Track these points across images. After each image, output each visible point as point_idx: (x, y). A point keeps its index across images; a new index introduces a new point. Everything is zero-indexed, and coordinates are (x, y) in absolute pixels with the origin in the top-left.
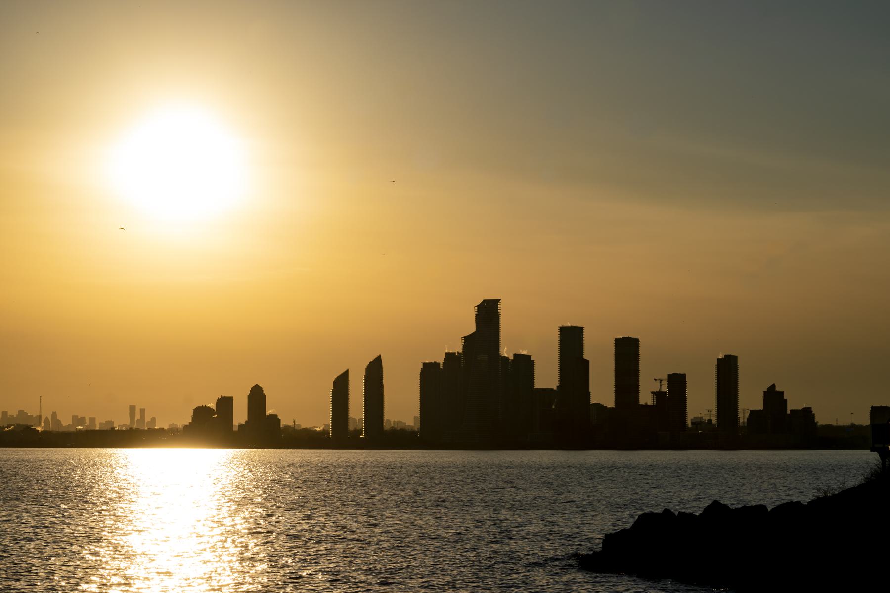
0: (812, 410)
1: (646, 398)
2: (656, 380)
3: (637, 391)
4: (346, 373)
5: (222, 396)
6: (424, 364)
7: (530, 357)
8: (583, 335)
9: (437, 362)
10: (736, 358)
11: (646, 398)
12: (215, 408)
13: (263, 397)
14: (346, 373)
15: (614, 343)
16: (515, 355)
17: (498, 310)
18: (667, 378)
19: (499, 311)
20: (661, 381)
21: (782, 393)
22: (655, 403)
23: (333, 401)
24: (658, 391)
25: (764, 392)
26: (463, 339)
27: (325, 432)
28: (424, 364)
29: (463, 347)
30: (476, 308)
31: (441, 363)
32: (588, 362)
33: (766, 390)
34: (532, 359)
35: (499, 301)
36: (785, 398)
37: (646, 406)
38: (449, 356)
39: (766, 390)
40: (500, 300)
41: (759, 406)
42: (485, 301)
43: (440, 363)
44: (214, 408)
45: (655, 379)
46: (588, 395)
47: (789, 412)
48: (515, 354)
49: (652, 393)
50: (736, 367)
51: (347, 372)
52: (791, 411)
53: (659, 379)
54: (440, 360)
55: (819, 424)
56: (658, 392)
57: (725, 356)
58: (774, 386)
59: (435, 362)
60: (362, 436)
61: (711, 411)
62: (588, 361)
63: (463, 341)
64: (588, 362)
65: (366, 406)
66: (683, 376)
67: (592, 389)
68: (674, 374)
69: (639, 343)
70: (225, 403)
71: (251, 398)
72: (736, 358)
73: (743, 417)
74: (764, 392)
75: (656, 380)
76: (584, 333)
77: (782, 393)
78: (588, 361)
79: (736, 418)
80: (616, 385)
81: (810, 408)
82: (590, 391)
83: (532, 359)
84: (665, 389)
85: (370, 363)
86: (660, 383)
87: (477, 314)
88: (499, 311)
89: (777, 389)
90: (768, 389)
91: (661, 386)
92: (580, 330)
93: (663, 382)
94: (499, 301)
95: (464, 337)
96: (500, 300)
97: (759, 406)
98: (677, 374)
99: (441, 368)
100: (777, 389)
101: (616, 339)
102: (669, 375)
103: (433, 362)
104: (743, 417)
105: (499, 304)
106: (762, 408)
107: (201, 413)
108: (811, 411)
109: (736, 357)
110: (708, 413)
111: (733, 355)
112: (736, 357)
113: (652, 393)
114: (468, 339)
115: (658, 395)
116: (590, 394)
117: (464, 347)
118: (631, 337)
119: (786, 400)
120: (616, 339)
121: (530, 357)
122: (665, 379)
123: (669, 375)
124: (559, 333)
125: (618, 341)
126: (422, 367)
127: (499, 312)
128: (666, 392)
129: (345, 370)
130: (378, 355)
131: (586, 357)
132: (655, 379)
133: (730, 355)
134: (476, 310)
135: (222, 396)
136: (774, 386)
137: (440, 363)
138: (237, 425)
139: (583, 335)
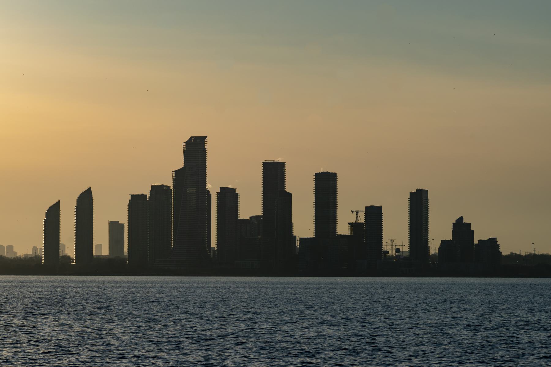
0: (497, 240)
2: (353, 212)
3: (335, 222)
4: (57, 205)
6: (132, 196)
7: (235, 189)
8: (284, 170)
14: (57, 205)
15: (314, 177)
16: (221, 188)
18: (364, 210)
19: (205, 147)
20: (357, 213)
21: (470, 224)
22: (352, 233)
23: (45, 230)
24: (354, 222)
25: (453, 224)
26: (174, 173)
27: (36, 258)
28: (132, 196)
30: (185, 144)
31: (148, 196)
32: (290, 195)
33: (455, 222)
35: (205, 137)
36: (472, 229)
37: (345, 236)
38: (157, 190)
39: (455, 222)
40: (207, 137)
41: (449, 237)
42: (191, 137)
43: (146, 196)
45: (352, 211)
46: (291, 225)
47: (476, 242)
48: (222, 187)
49: (349, 224)
51: (59, 202)
52: (479, 241)
54: (147, 192)
55: (503, 254)
57: (417, 190)
58: (462, 218)
59: (143, 194)
60: (72, 263)
61: (393, 241)
62: (291, 194)
63: (174, 175)
64: (290, 195)
65: (77, 235)
67: (293, 220)
68: (371, 206)
69: (337, 177)
73: (434, 247)
74: (453, 224)
75: (353, 212)
76: (285, 168)
77: (470, 224)
78: (291, 194)
79: (427, 248)
80: (315, 217)
81: (496, 238)
82: (292, 222)
84: (362, 220)
86: (357, 214)
87: (184, 150)
88: (205, 147)
89: (465, 221)
90: (456, 221)
91: (357, 217)
92: (282, 165)
93: (359, 214)
94: (205, 137)
96: (207, 137)
97: (449, 237)
98: (373, 206)
99: (148, 199)
100: (465, 221)
102: (366, 207)
103: (140, 194)
104: (434, 247)
105: (205, 140)
106: (452, 240)
108: (497, 242)
109: (427, 191)
110: (391, 242)
112: (427, 191)
113: (349, 224)
114: (177, 172)
115: (355, 226)
116: (292, 225)
117: (175, 181)
119: (473, 231)
121: (235, 189)
122: (361, 211)
123: (366, 208)
124: (262, 168)
125: (317, 175)
126: (130, 199)
127: (206, 148)
128: (363, 223)
129: (57, 201)
130: (88, 187)
131: (288, 189)
132: (352, 211)
133: (422, 190)
134: (185, 147)
136: (462, 218)
137: (146, 196)
138: (17, 255)
139: (284, 170)
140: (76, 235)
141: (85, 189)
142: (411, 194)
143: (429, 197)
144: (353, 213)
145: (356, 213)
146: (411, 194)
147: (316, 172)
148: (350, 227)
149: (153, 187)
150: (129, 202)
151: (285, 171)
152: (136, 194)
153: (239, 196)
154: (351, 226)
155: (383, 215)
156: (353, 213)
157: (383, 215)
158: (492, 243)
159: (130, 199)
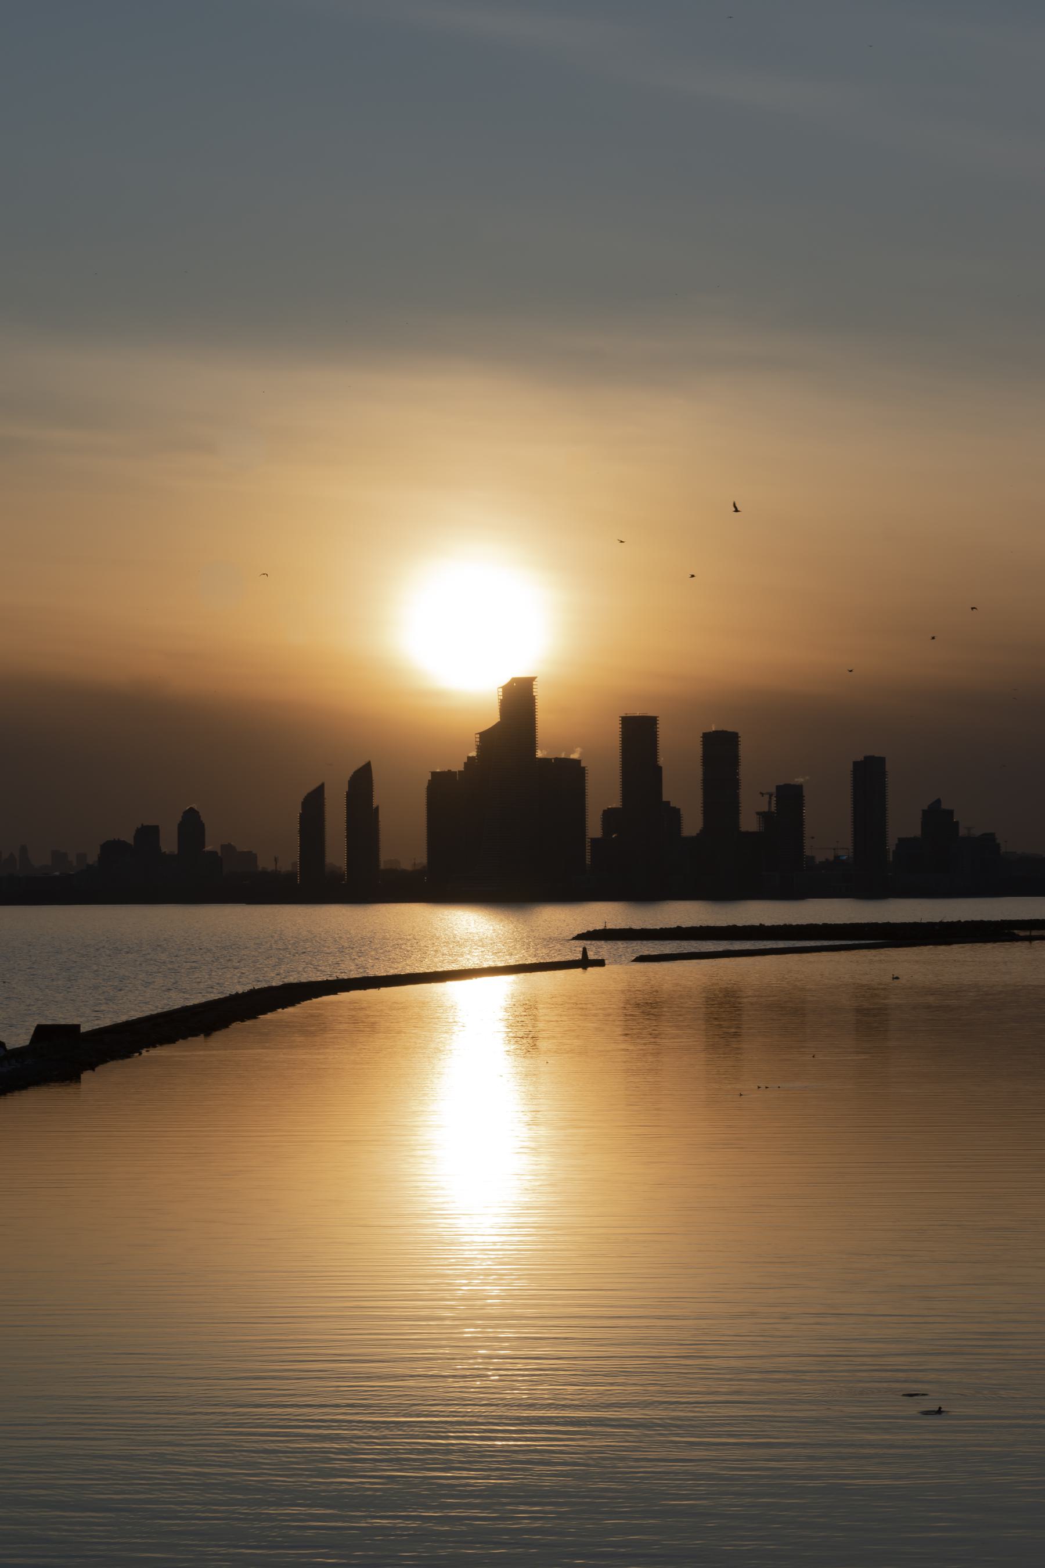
1: (749, 822)
2: (762, 794)
5: (142, 825)
9: (453, 770)
10: (882, 760)
11: (749, 822)
12: (133, 844)
13: (201, 826)
17: (532, 692)
23: (303, 832)
24: (766, 809)
25: (923, 811)
26: (478, 736)
28: (434, 774)
29: (478, 749)
30: (501, 690)
33: (926, 808)
34: (582, 765)
37: (747, 833)
42: (514, 680)
44: (133, 844)
45: (761, 793)
49: (758, 813)
50: (883, 774)
53: (767, 793)
56: (764, 812)
58: (938, 801)
59: (449, 771)
63: (478, 740)
64: (661, 768)
66: (799, 788)
69: (740, 739)
70: (148, 834)
71: (182, 826)
72: (882, 760)
74: (923, 811)
75: (762, 794)
76: (658, 726)
77: (950, 813)
83: (582, 765)
85: (355, 773)
88: (534, 694)
94: (533, 679)
95: (483, 735)
96: (536, 677)
100: (945, 806)
101: (704, 734)
102: (778, 787)
103: (446, 770)
107: (112, 849)
111: (876, 756)
113: (758, 813)
115: (764, 816)
118: (726, 731)
119: (957, 823)
120: (704, 734)
123: (778, 787)
124: (621, 726)
126: (430, 779)
129: (320, 783)
130: (367, 761)
131: (662, 760)
132: (761, 793)
135: (142, 825)
136: (938, 801)
139: (657, 728)
140: (347, 836)
141: (361, 763)
142: (855, 764)
143: (889, 767)
144: (763, 796)
145: (768, 796)
146: (855, 764)
147: (705, 732)
148: (760, 818)
149: (469, 758)
150: (429, 783)
151: (658, 730)
152: (438, 770)
153: (586, 772)
154: (761, 817)
155: (804, 798)
156: (763, 796)
157: (804, 798)
158: (988, 840)
159: (430, 779)
